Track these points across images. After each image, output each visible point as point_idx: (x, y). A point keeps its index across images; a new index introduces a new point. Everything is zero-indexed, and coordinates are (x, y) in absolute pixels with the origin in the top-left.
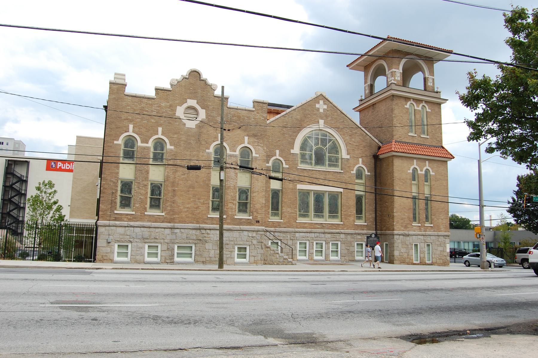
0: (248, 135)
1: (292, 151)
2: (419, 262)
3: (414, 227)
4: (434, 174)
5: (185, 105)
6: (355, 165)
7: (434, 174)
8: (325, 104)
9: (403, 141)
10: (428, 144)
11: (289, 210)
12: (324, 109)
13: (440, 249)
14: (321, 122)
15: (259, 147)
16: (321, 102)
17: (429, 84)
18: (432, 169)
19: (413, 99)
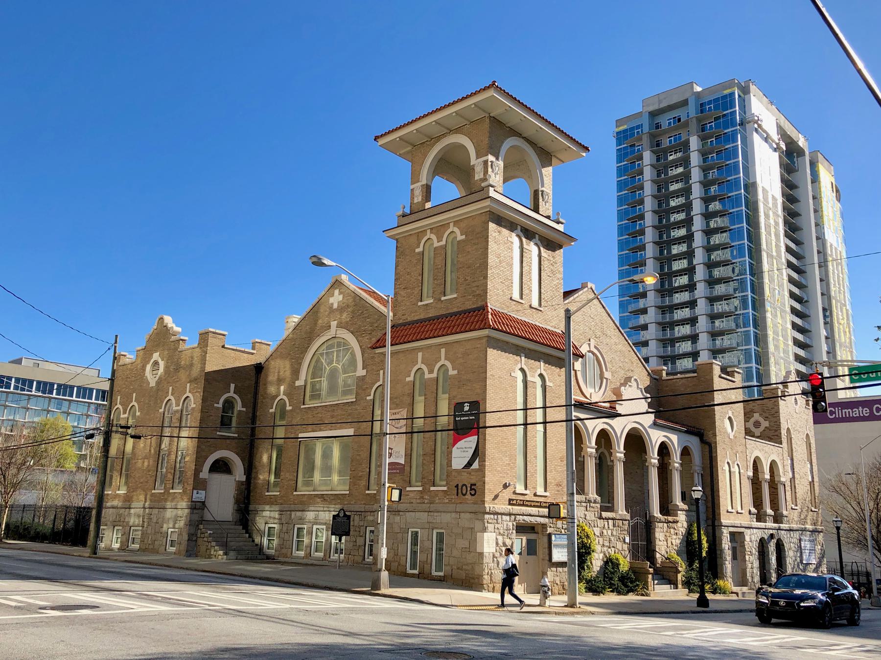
0: (190, 382)
1: (298, 383)
2: (416, 572)
3: (412, 495)
4: (455, 372)
5: (152, 361)
6: (374, 384)
7: (455, 372)
8: (333, 295)
9: (409, 319)
10: (455, 310)
11: (287, 475)
12: (332, 304)
13: (462, 543)
14: (334, 324)
15: (197, 394)
16: (337, 292)
17: (477, 177)
18: (452, 362)
19: (431, 229)
